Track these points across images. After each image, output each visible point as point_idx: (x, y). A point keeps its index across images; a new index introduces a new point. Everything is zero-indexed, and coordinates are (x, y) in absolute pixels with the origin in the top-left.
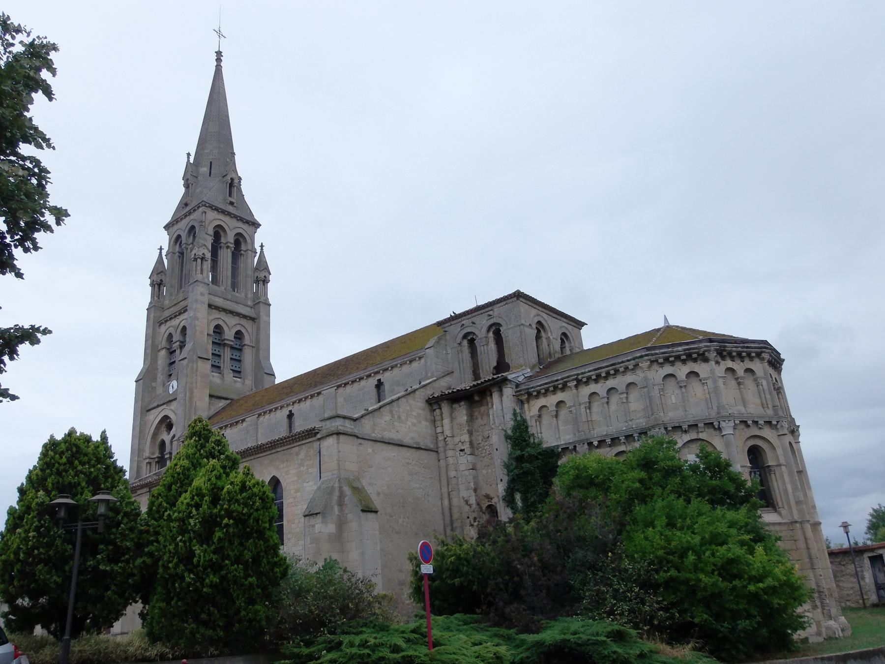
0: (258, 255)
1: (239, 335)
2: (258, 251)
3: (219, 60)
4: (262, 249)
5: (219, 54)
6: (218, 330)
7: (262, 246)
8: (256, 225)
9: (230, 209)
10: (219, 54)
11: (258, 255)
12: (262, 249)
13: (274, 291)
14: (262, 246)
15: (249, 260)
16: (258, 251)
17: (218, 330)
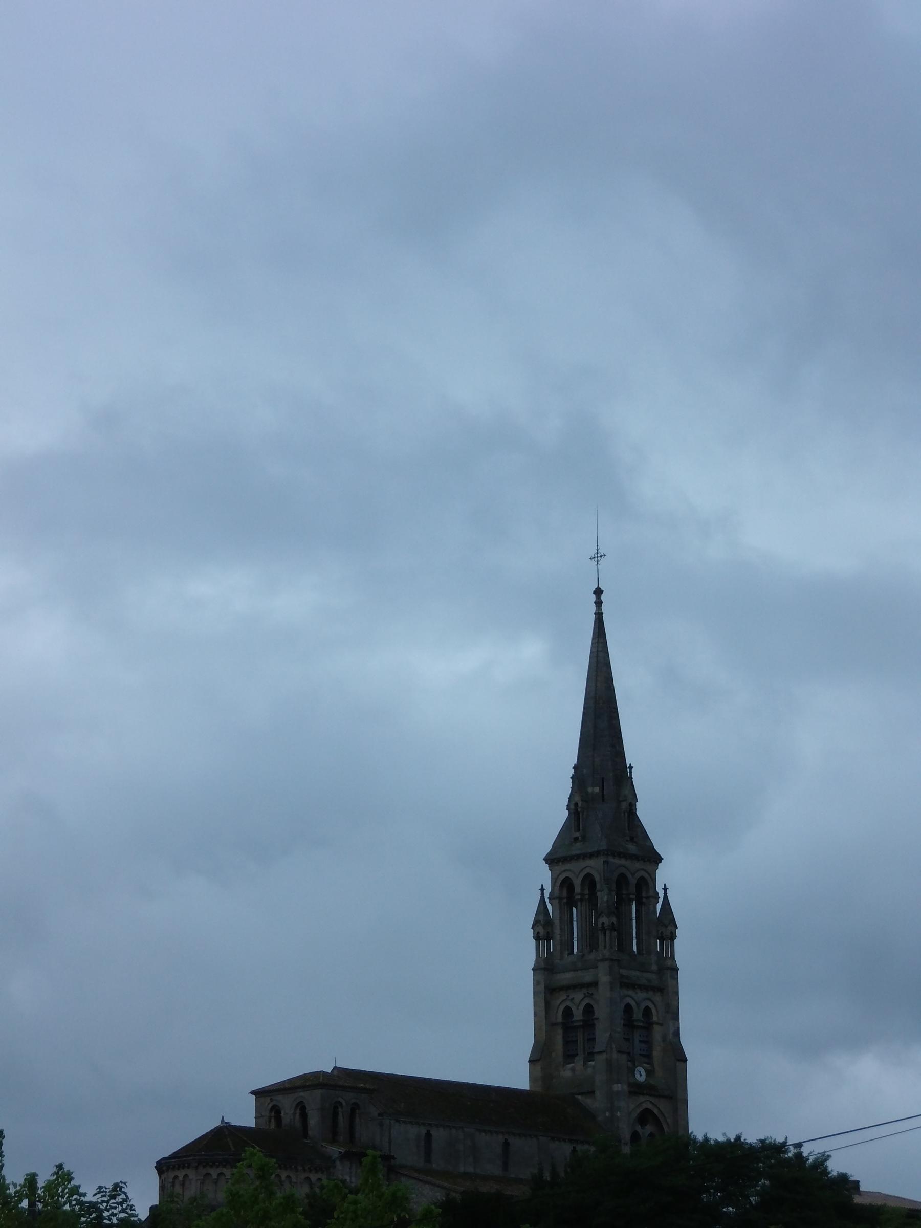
0: (661, 900)
1: (647, 1012)
2: (661, 895)
3: (599, 603)
4: (665, 894)
5: (598, 592)
6: (628, 1009)
7: (665, 889)
8: (657, 859)
9: (632, 848)
10: (598, 592)
11: (661, 900)
12: (665, 894)
13: (684, 951)
14: (665, 889)
15: (651, 906)
16: (661, 895)
17: (628, 1009)
